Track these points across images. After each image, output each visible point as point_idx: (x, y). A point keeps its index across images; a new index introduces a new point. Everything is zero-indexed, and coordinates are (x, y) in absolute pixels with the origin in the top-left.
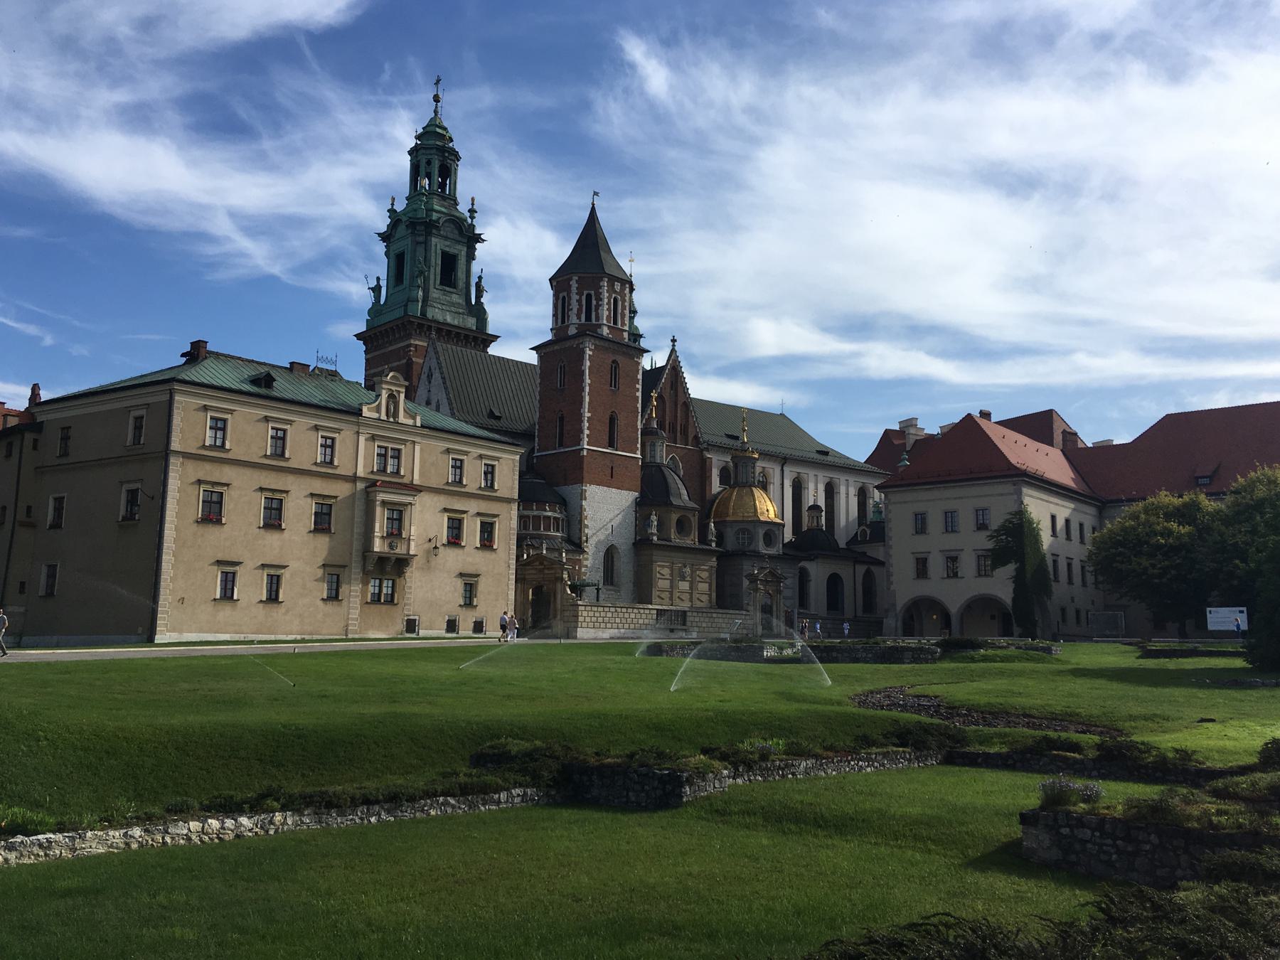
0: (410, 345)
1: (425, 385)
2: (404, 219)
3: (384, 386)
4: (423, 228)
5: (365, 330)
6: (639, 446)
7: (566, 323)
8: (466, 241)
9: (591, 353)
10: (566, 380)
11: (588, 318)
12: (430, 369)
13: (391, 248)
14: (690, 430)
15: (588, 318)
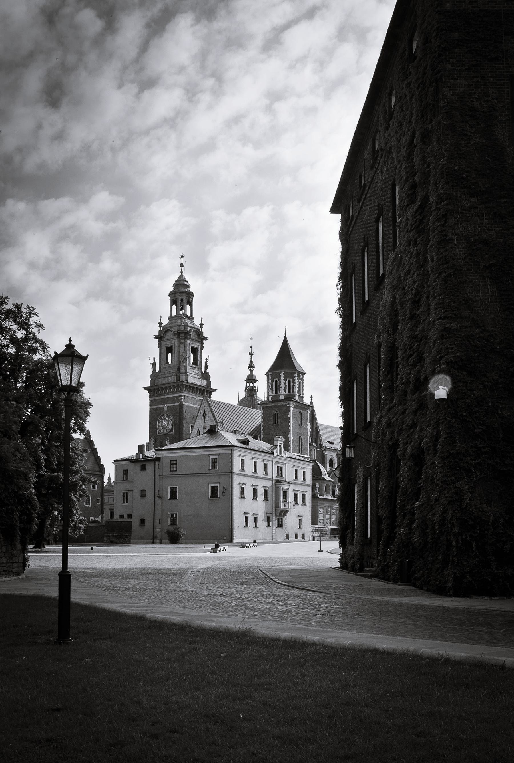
0: (182, 396)
1: (201, 419)
2: (173, 330)
3: (279, 442)
4: (184, 335)
5: (148, 385)
6: (309, 452)
7: (278, 394)
8: (200, 340)
9: (292, 409)
10: (279, 421)
11: (289, 392)
12: (205, 412)
13: (163, 343)
14: (318, 441)
15: (289, 392)
